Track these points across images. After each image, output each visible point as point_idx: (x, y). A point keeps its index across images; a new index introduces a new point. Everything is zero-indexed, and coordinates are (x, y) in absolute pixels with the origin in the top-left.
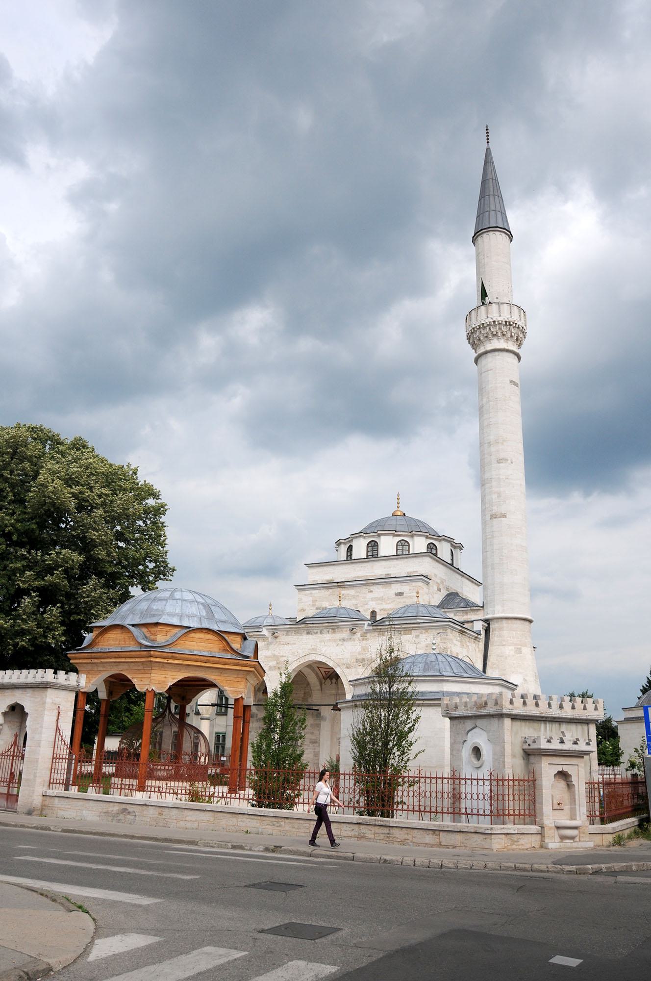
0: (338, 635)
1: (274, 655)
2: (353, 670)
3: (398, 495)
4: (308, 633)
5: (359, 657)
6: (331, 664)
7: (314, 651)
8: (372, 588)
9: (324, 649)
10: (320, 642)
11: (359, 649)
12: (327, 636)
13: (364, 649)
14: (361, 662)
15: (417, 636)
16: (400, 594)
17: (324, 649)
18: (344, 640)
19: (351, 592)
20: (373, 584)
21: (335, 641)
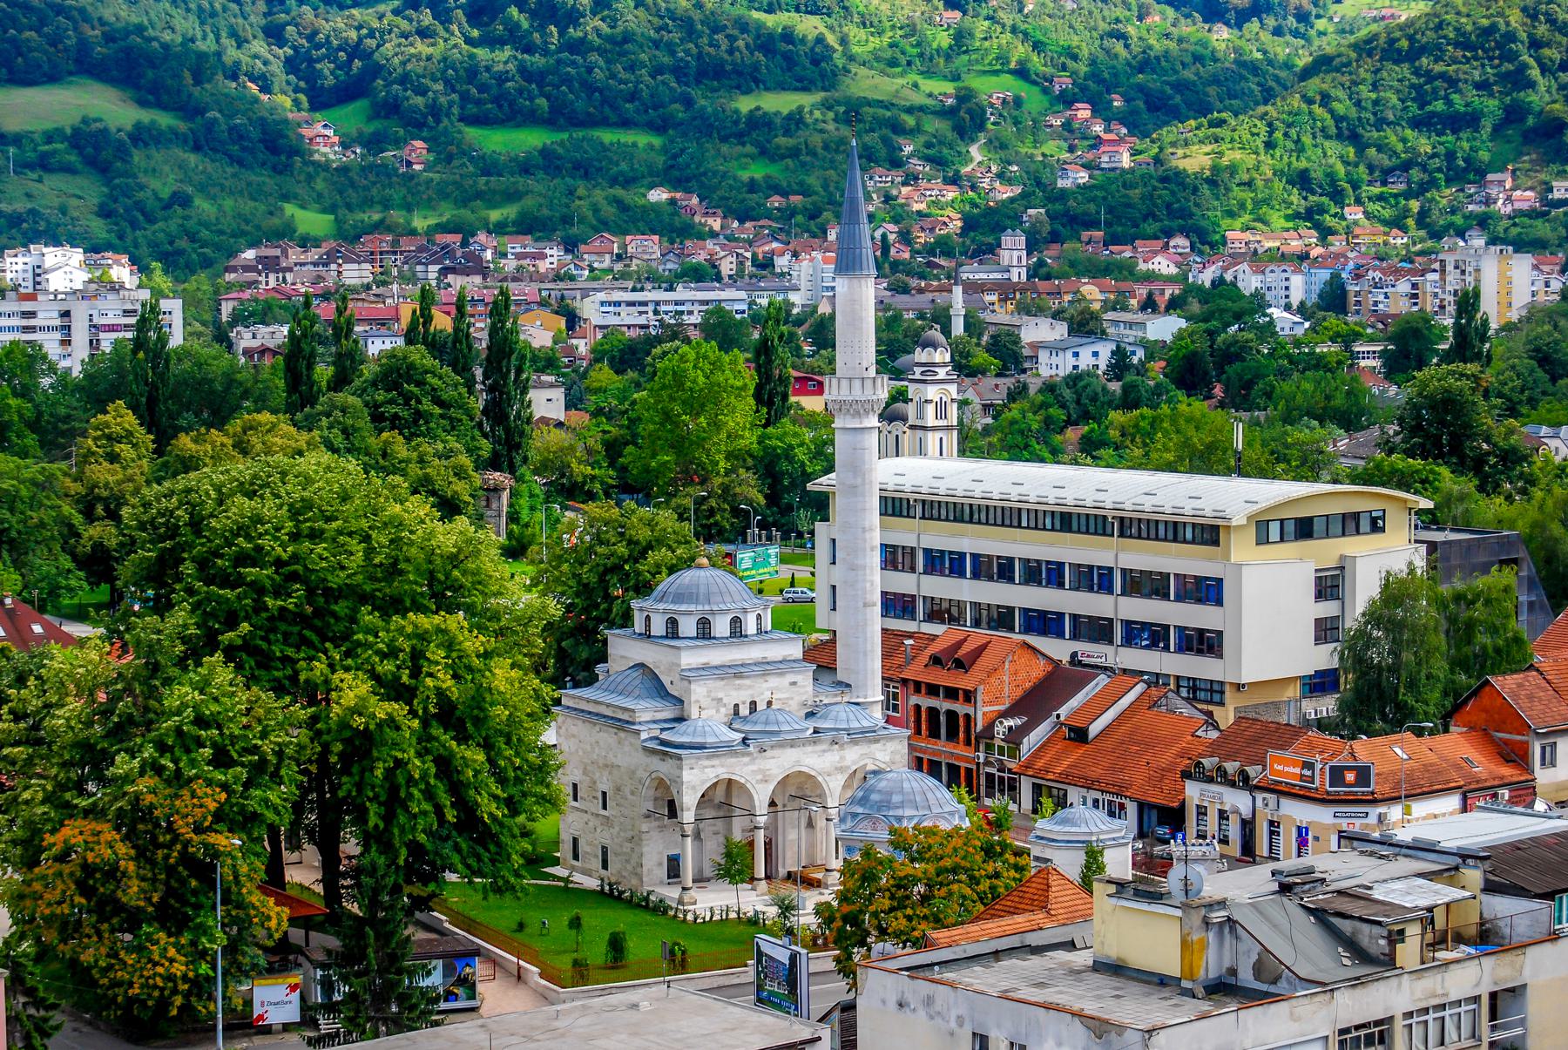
0: (819, 748)
7: (798, 763)
13: (842, 758)
14: (841, 769)
16: (794, 683)
19: (747, 682)
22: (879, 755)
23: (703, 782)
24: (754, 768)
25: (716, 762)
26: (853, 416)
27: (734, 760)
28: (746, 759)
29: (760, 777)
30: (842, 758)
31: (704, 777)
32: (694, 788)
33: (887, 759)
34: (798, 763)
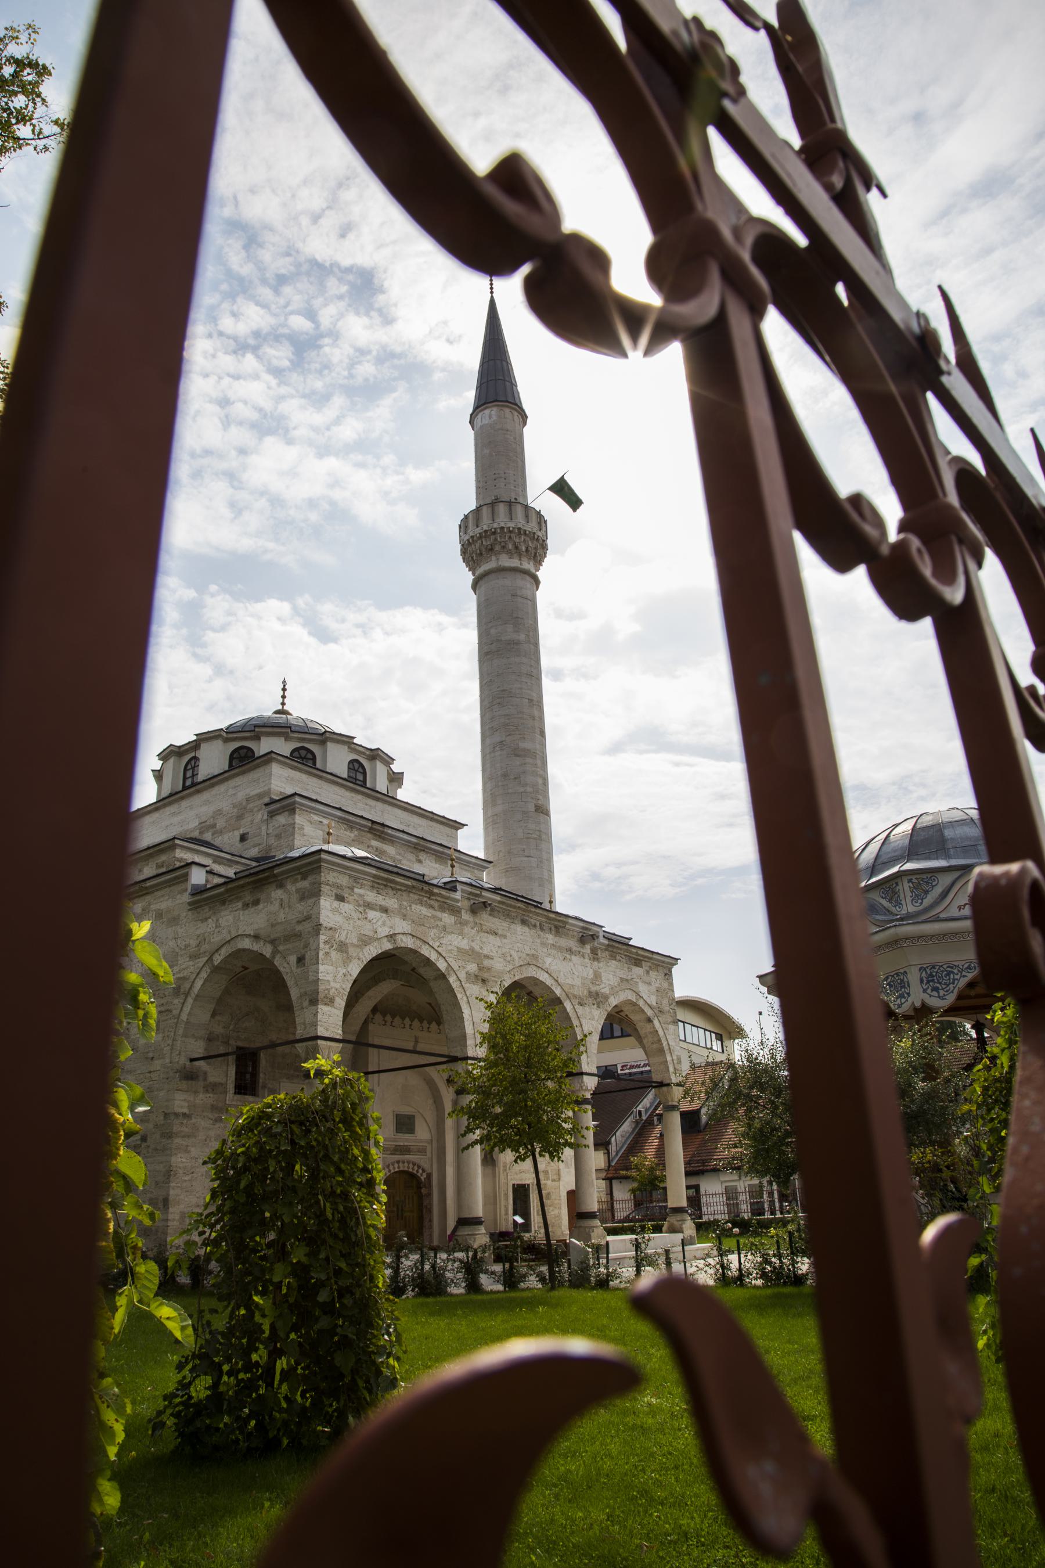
0: (563, 942)
1: (472, 949)
2: (587, 1009)
3: (284, 683)
4: (524, 922)
5: (594, 989)
6: (558, 992)
7: (533, 960)
8: (423, 856)
9: (549, 960)
10: (543, 944)
11: (591, 976)
12: (550, 938)
13: (597, 976)
14: (598, 998)
15: (648, 972)
17: (549, 960)
18: (570, 951)
20: (424, 850)
21: (560, 949)
22: (643, 989)
23: (365, 941)
24: (464, 944)
25: (391, 903)
26: (510, 554)
27: (425, 911)
28: (447, 919)
29: (472, 967)
30: (597, 976)
31: (367, 930)
32: (342, 947)
33: (653, 1000)
34: (533, 960)
